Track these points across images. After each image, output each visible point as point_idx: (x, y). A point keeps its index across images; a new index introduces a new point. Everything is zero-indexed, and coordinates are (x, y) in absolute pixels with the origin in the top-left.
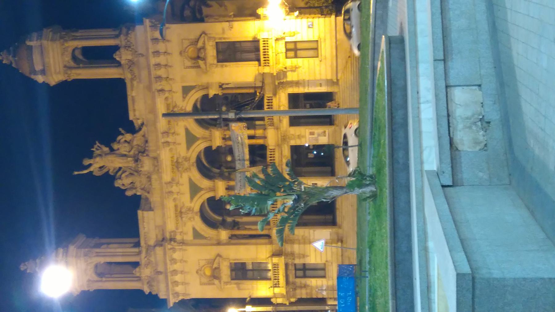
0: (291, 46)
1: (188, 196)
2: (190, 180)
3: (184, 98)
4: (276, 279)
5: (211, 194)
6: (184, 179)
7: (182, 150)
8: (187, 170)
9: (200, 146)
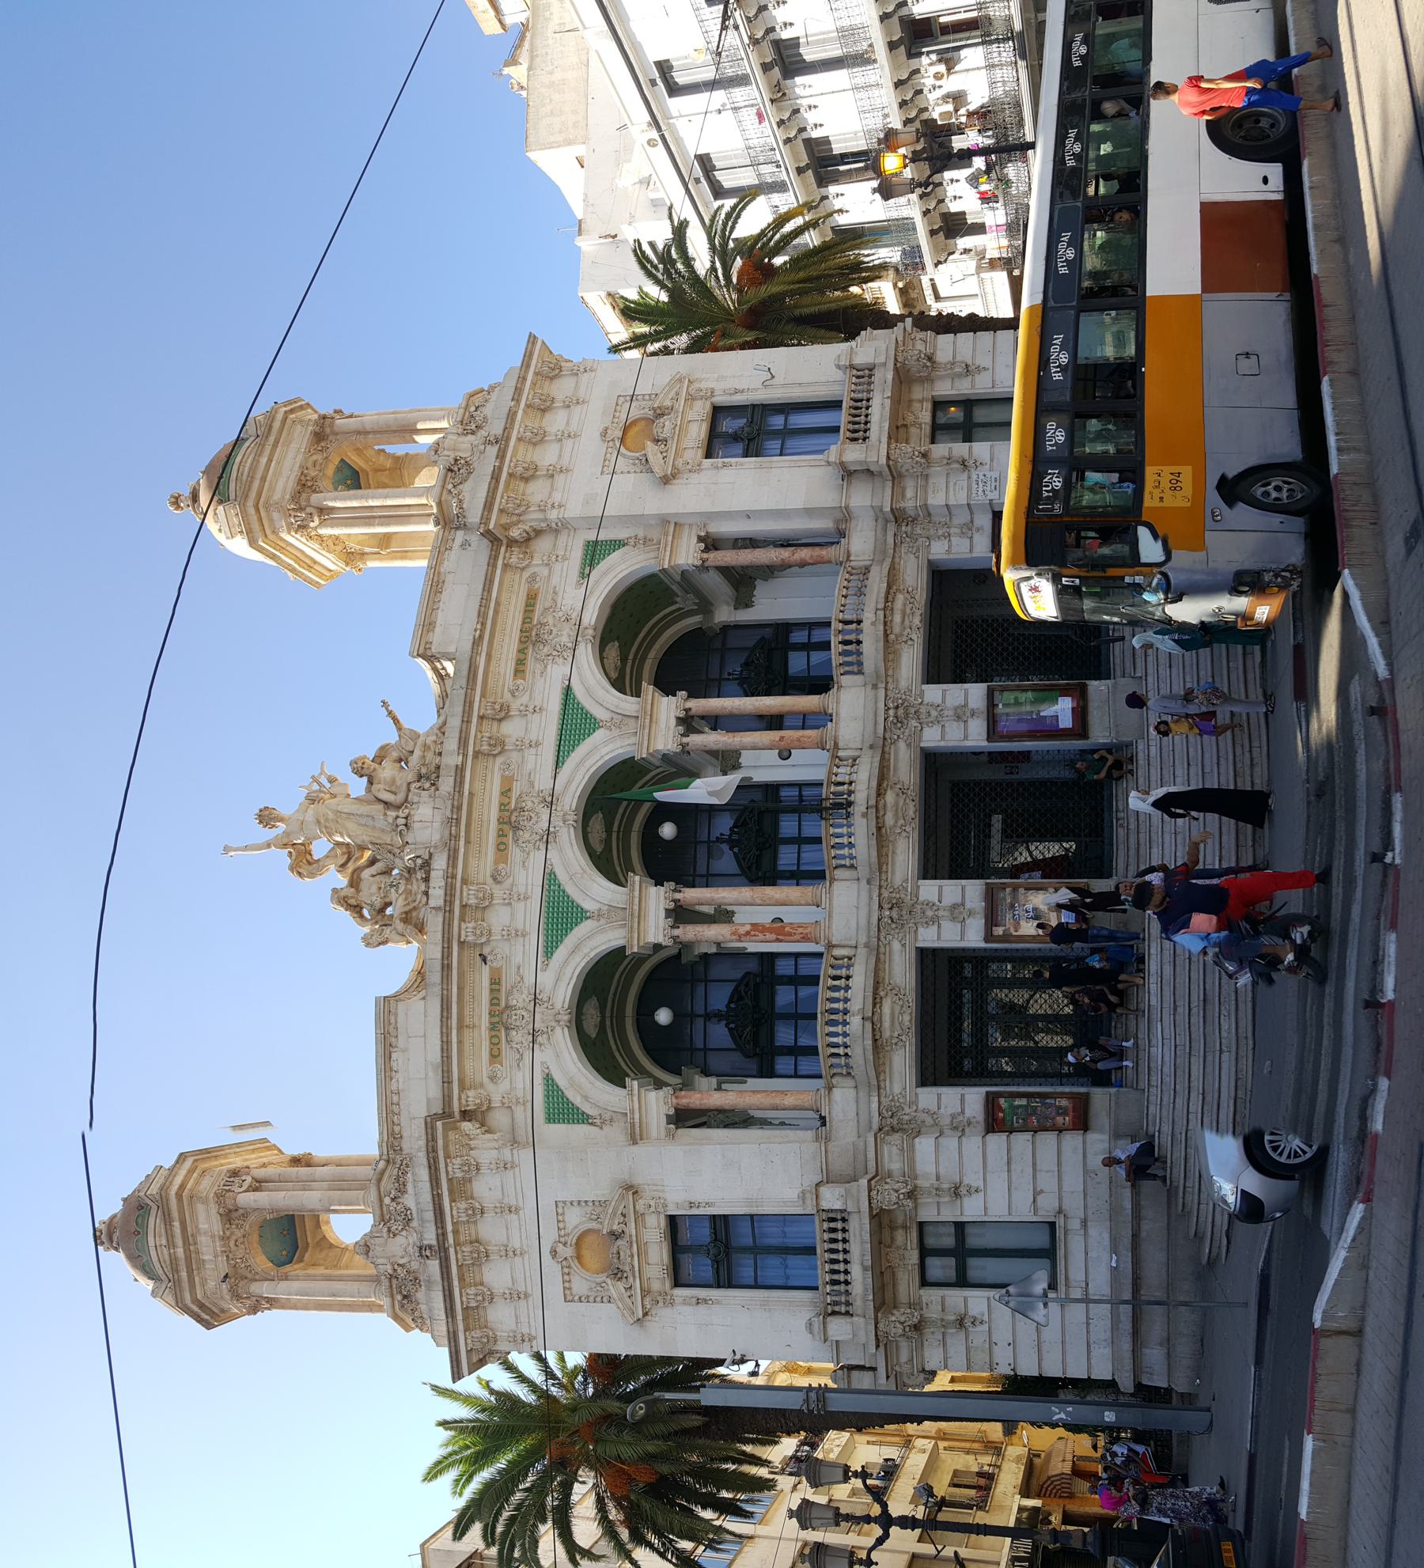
2: (550, 878)
4: (840, 1280)
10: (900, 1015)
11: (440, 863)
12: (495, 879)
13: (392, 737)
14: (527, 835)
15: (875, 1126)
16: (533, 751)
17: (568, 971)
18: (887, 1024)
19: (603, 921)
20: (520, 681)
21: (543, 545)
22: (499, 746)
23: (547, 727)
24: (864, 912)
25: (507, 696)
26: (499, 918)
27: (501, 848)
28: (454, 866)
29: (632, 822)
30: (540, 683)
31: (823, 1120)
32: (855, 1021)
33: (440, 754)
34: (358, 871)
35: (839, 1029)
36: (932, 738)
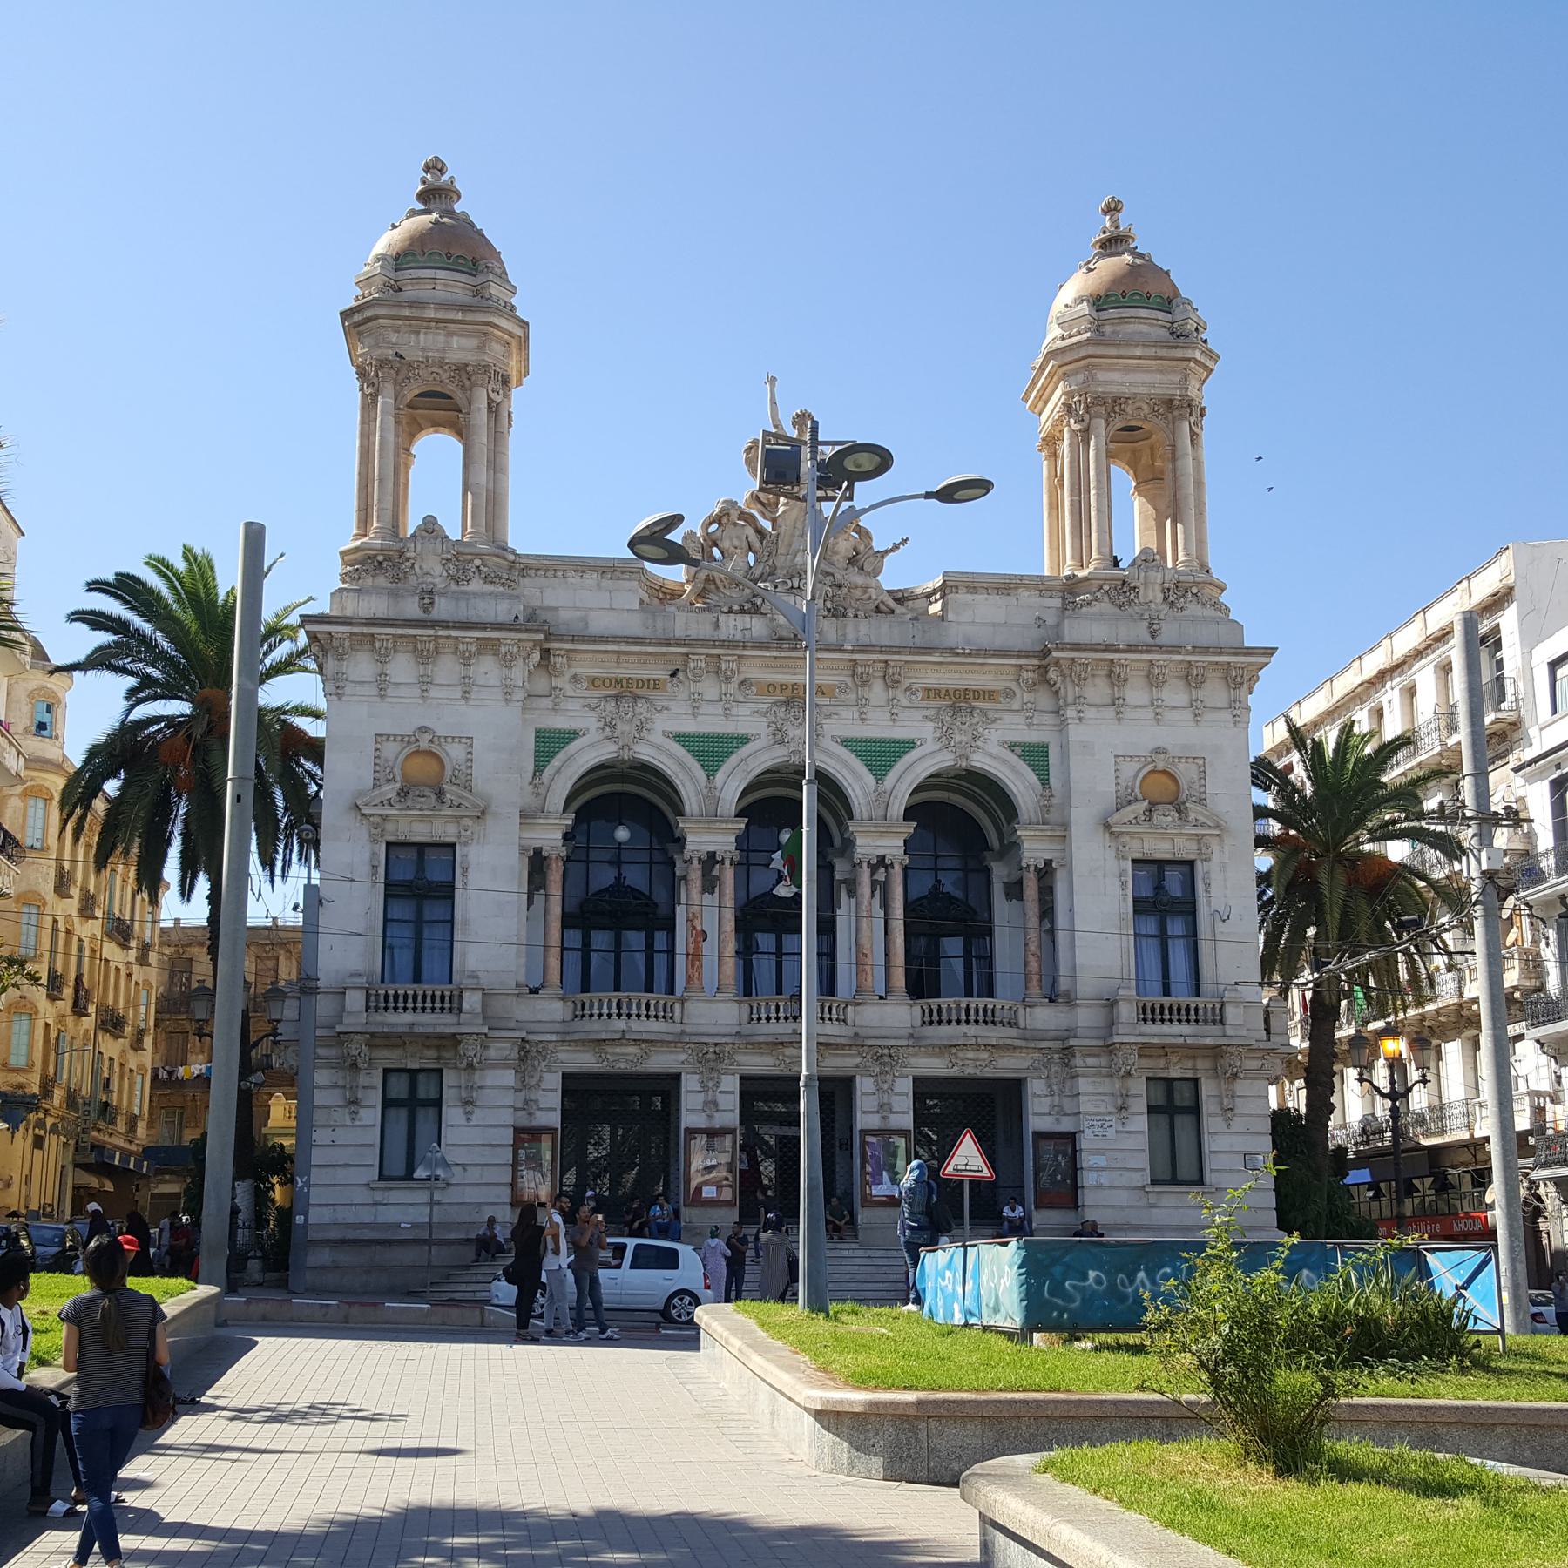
0: (1182, 1096)
1: (689, 727)
2: (744, 740)
3: (1012, 746)
5: (691, 802)
7: (844, 723)
8: (779, 737)
9: (857, 782)
10: (624, 1060)
11: (757, 627)
12: (742, 683)
13: (877, 545)
14: (781, 714)
15: (530, 1037)
16: (856, 715)
17: (664, 758)
18: (618, 1050)
19: (705, 791)
20: (920, 694)
22: (864, 682)
23: (879, 728)
24: (714, 1030)
25: (907, 683)
26: (709, 688)
27: (771, 688)
28: (753, 648)
30: (918, 715)
31: (534, 991)
32: (621, 1024)
33: (856, 616)
34: (750, 520)
35: (615, 1011)
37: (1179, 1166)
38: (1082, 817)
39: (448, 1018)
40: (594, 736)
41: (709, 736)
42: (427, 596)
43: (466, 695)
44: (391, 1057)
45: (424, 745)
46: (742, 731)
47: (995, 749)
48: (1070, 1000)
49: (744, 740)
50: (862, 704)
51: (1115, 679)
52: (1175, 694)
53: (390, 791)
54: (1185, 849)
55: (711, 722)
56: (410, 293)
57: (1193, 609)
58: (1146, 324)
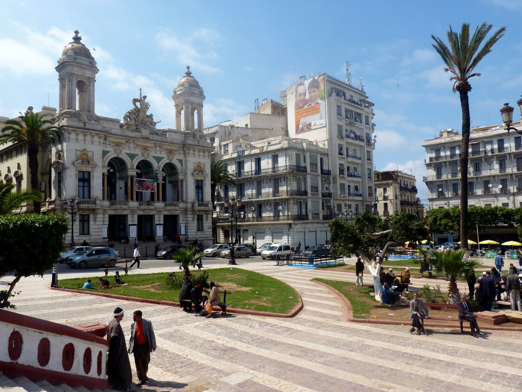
1: (128, 152)
2: (137, 155)
3: (178, 159)
5: (129, 166)
6: (138, 151)
7: (153, 153)
8: (143, 155)
9: (155, 164)
10: (119, 212)
21: (182, 152)
26: (132, 145)
27: (141, 146)
29: (145, 167)
36: (156, 216)
37: (200, 228)
38: (189, 172)
39: (94, 205)
40: (112, 152)
41: (131, 154)
42: (85, 124)
43: (92, 143)
44: (81, 212)
45: (85, 152)
46: (137, 153)
47: (175, 160)
48: (187, 203)
49: (137, 155)
50: (156, 150)
51: (194, 151)
52: (201, 154)
53: (80, 161)
54: (202, 178)
55: (132, 152)
56: (78, 61)
57: (203, 140)
58: (196, 91)
